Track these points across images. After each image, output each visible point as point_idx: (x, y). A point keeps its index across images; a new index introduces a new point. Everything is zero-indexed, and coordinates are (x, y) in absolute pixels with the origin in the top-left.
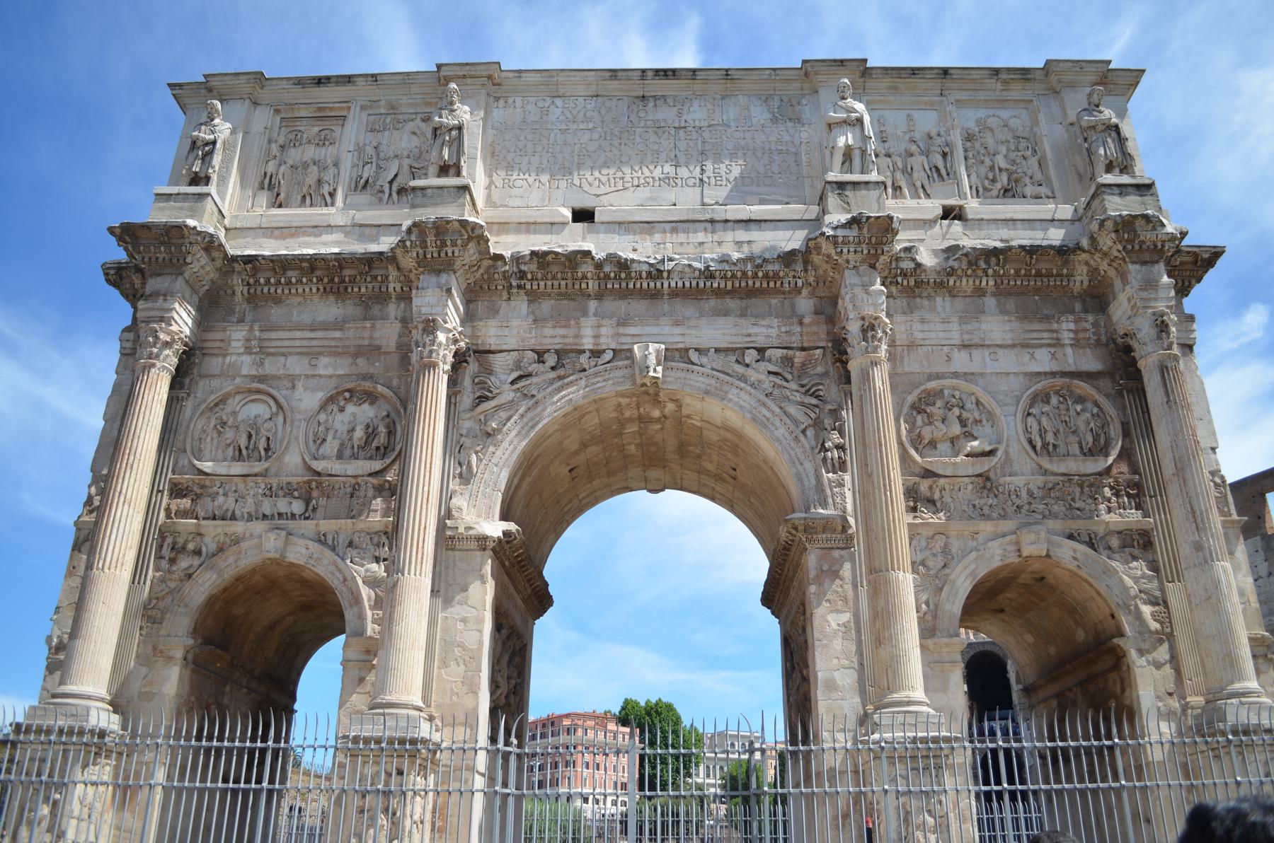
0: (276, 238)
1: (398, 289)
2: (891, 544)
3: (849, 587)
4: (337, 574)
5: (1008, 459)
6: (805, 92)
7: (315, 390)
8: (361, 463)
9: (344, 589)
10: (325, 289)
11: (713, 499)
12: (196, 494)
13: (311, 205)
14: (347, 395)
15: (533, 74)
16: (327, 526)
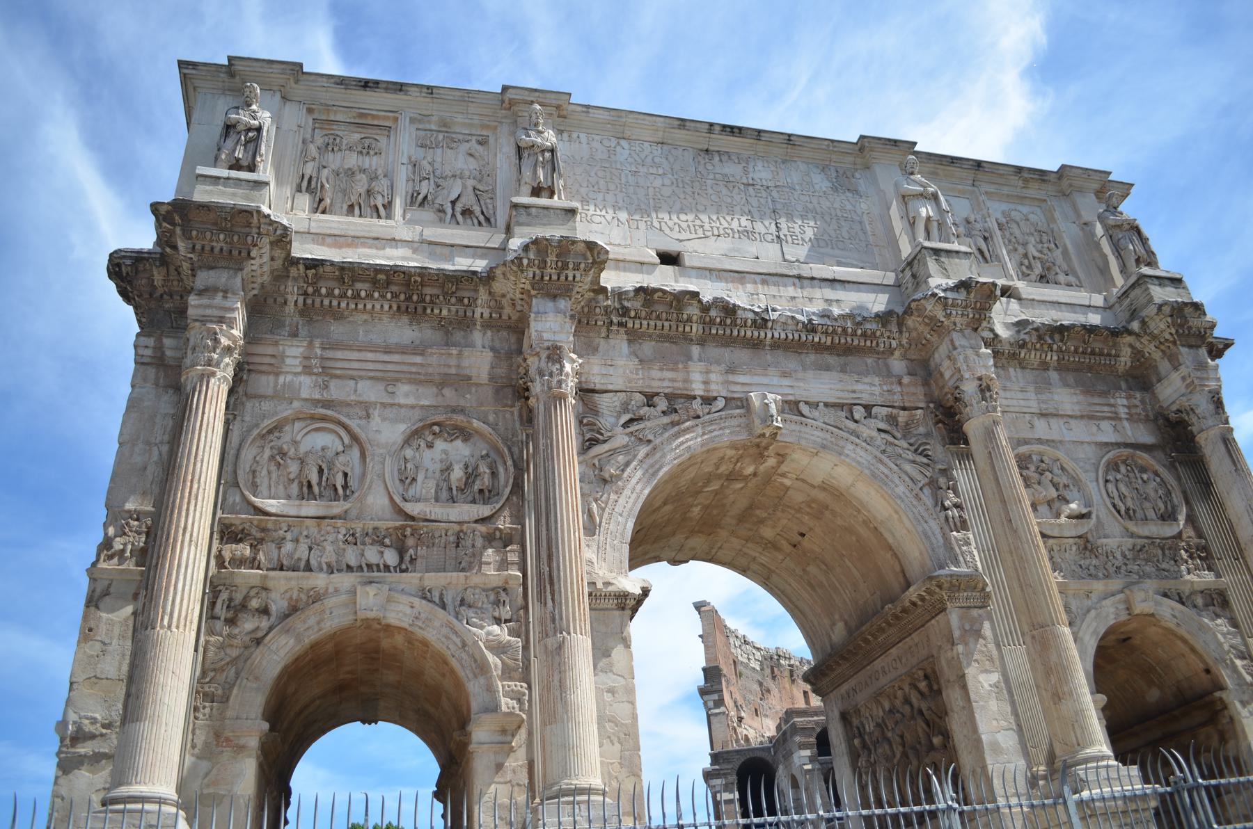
0: (329, 246)
1: (486, 315)
2: (1051, 598)
3: (992, 647)
4: (454, 637)
6: (858, 167)
7: (396, 421)
8: (467, 507)
9: (464, 656)
10: (399, 308)
11: (743, 571)
12: (255, 539)
13: (361, 216)
14: (436, 428)
15: (601, 112)
16: (434, 580)
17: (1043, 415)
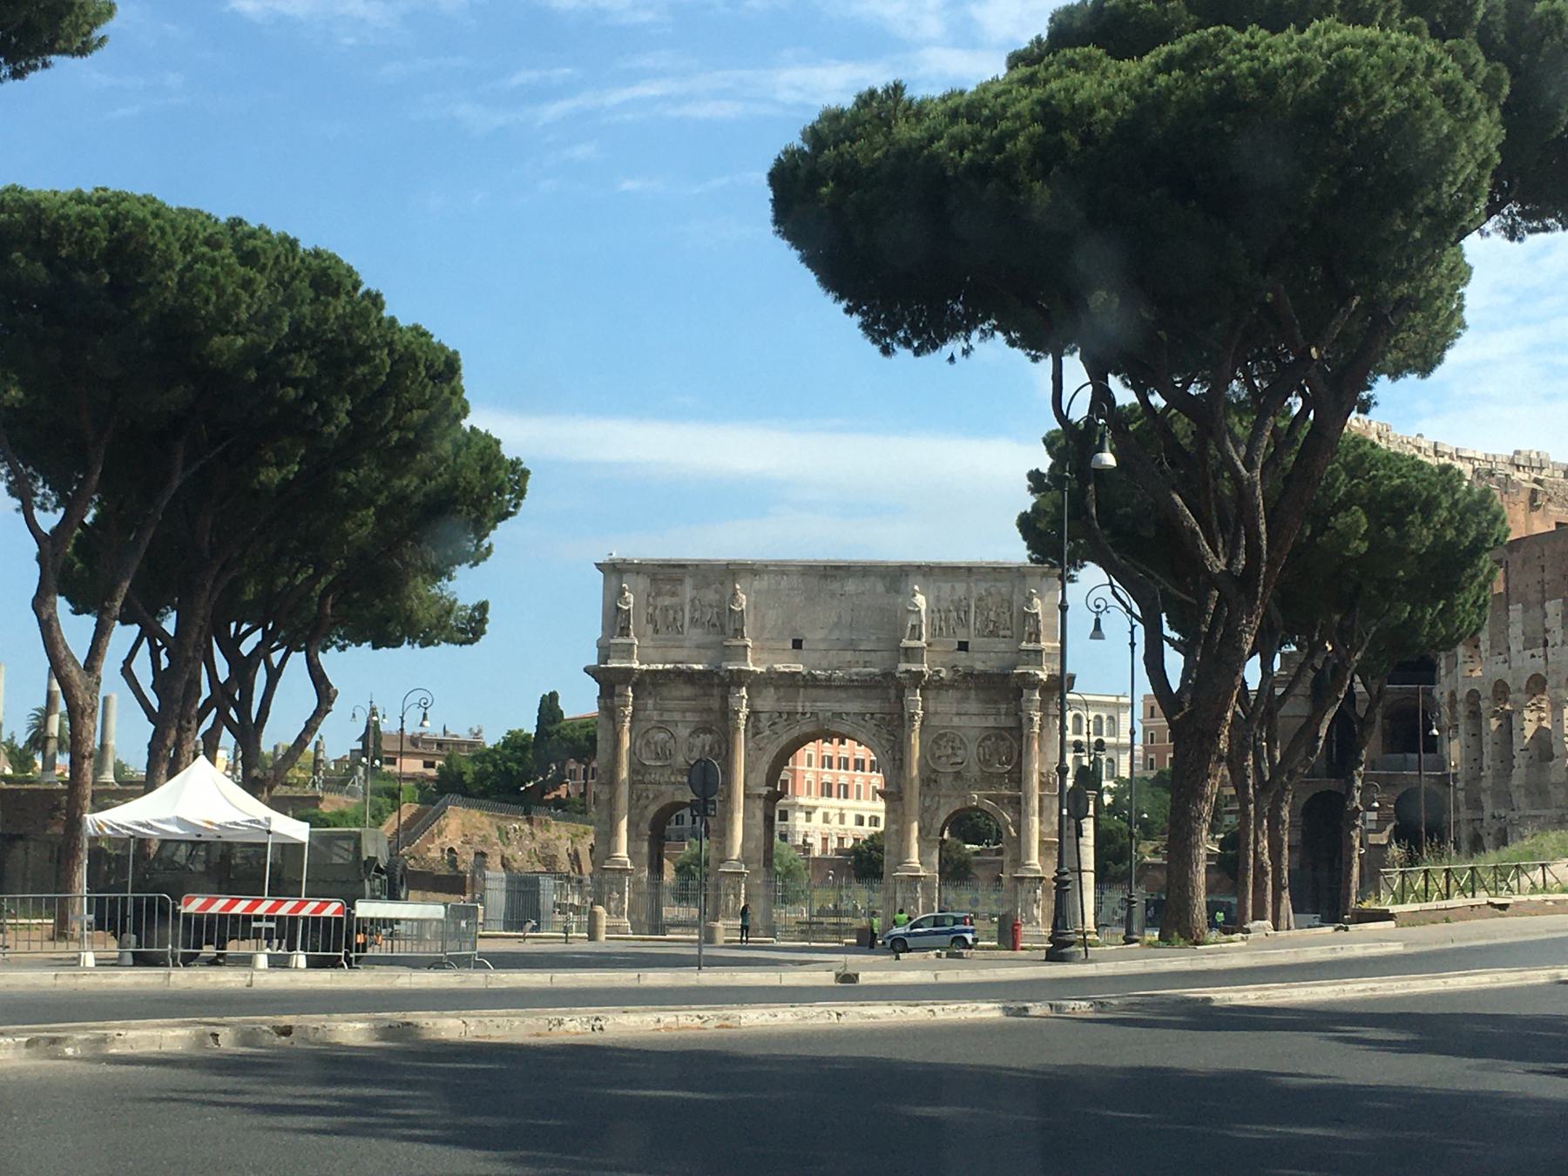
5: (968, 766)
7: (686, 728)
17: (958, 714)
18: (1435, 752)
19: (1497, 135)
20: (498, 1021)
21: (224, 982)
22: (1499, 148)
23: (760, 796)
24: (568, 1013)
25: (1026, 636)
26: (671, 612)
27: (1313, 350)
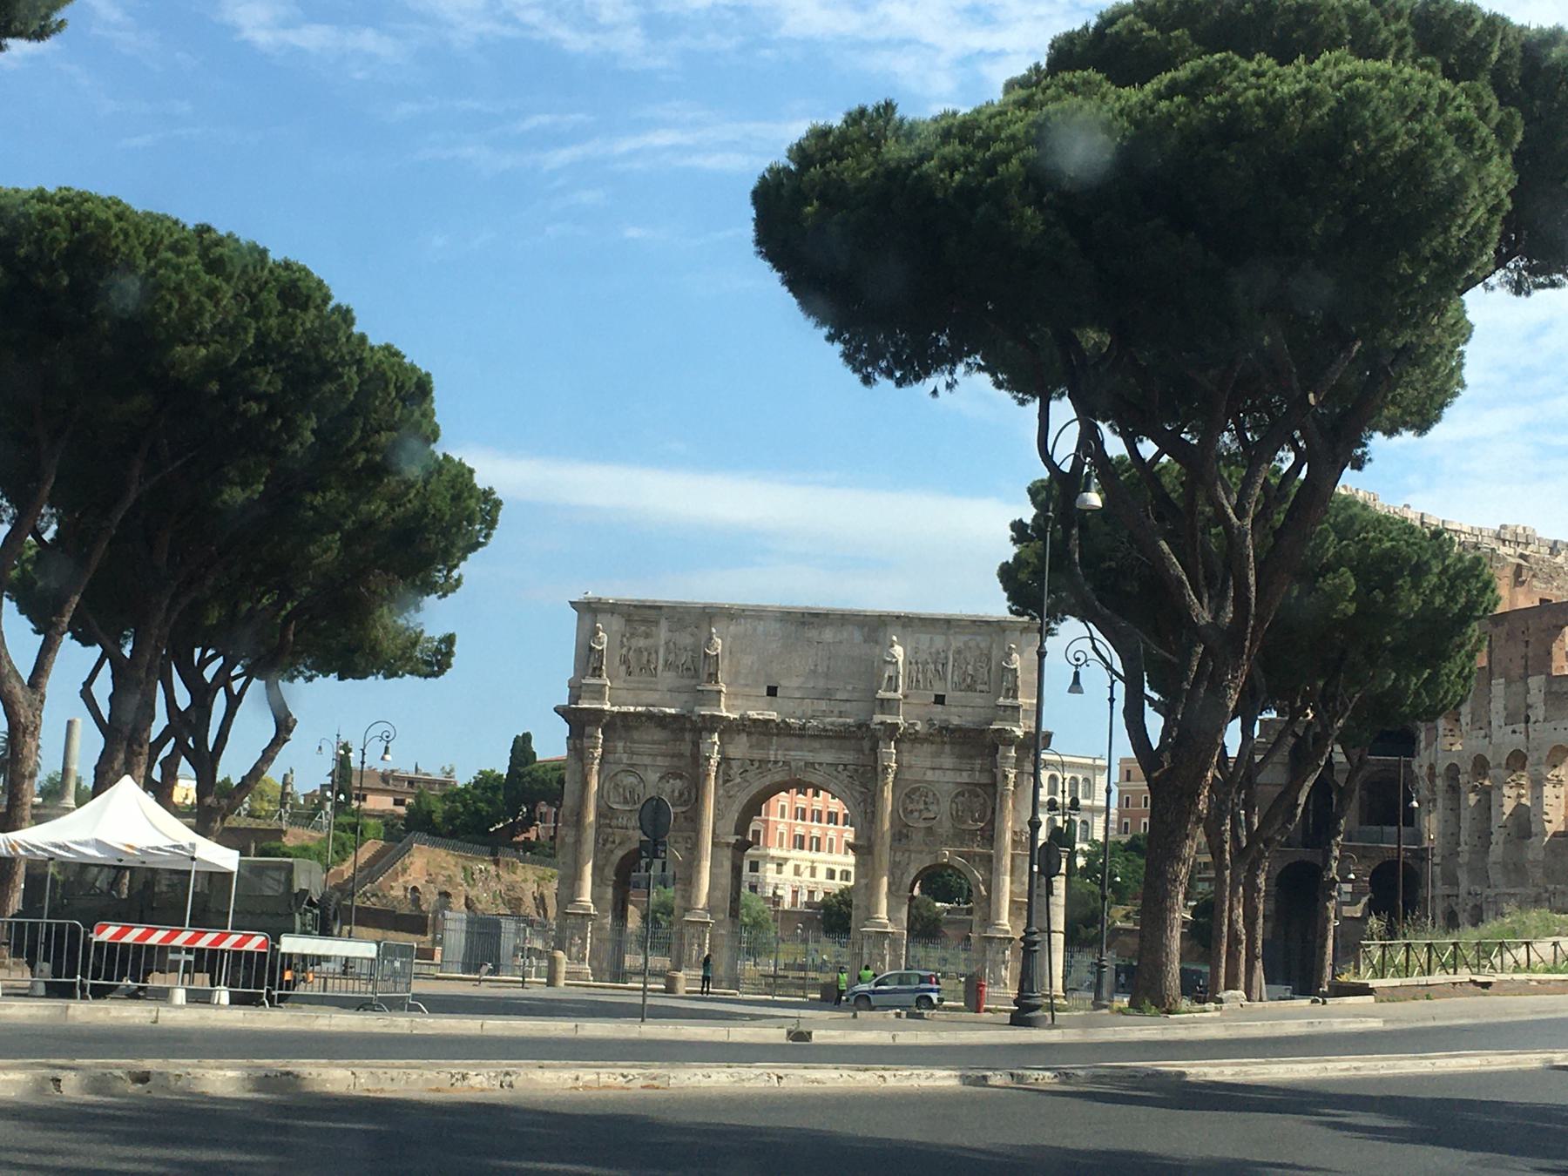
5: (940, 821)
7: (656, 772)
17: (934, 769)
18: (1413, 826)
19: (1509, 181)
20: (394, 1073)
21: (127, 1018)
22: (1509, 194)
23: (728, 844)
24: (475, 1067)
25: (1003, 692)
26: (646, 654)
27: (1311, 396)
